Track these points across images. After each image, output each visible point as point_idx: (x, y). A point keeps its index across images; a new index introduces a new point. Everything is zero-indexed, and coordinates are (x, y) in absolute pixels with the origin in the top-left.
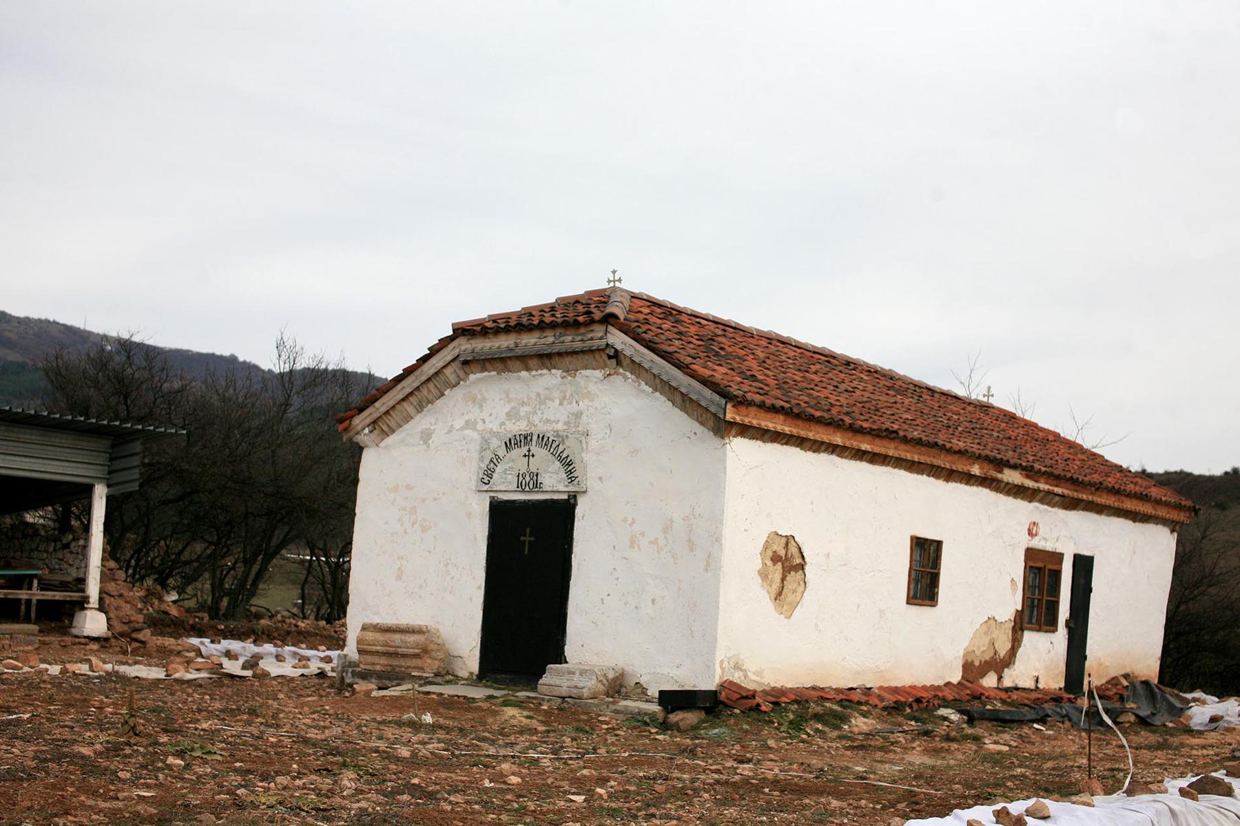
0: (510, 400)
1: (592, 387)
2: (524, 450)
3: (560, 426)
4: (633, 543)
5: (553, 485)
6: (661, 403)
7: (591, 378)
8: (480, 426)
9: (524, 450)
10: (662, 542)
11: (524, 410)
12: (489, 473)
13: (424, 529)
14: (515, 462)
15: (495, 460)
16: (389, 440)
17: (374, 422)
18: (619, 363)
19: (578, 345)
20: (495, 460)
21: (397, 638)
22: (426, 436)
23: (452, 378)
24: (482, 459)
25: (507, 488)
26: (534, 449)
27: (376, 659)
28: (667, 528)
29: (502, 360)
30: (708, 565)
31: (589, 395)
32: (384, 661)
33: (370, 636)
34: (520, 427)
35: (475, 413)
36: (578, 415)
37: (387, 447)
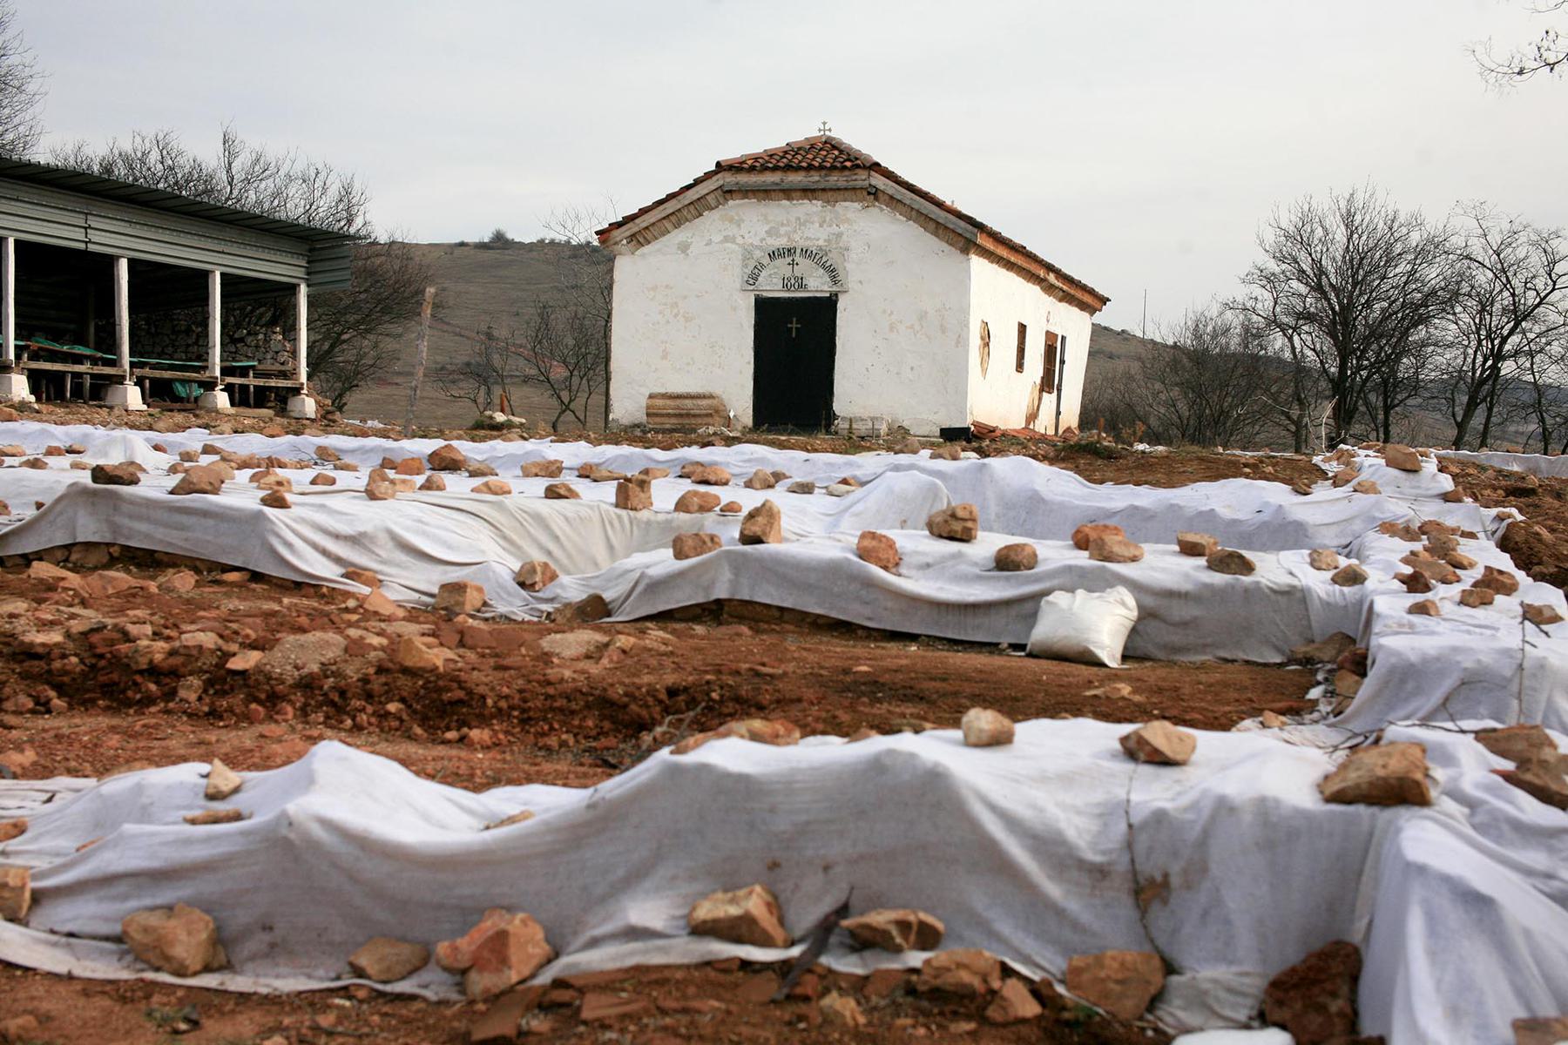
0: (768, 222)
1: (850, 215)
2: (789, 260)
3: (821, 243)
4: (892, 328)
5: (817, 285)
6: (914, 230)
7: (850, 210)
8: (739, 240)
9: (789, 260)
10: (917, 327)
11: (783, 230)
12: (754, 278)
13: (687, 320)
14: (782, 267)
15: (759, 267)
16: (646, 249)
17: (633, 235)
18: (876, 199)
19: (842, 184)
20: (759, 267)
21: (688, 403)
22: (684, 248)
23: (713, 203)
24: (746, 266)
25: (772, 287)
26: (797, 259)
27: (665, 420)
28: (923, 316)
29: (766, 191)
30: (958, 342)
31: (848, 220)
32: (673, 421)
33: (660, 402)
34: (782, 242)
35: (732, 230)
36: (839, 235)
37: (643, 255)
